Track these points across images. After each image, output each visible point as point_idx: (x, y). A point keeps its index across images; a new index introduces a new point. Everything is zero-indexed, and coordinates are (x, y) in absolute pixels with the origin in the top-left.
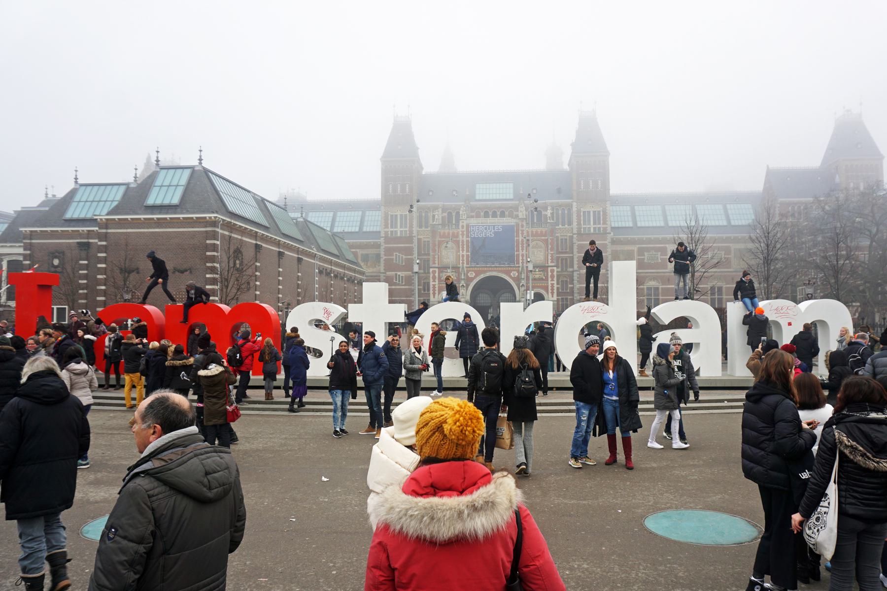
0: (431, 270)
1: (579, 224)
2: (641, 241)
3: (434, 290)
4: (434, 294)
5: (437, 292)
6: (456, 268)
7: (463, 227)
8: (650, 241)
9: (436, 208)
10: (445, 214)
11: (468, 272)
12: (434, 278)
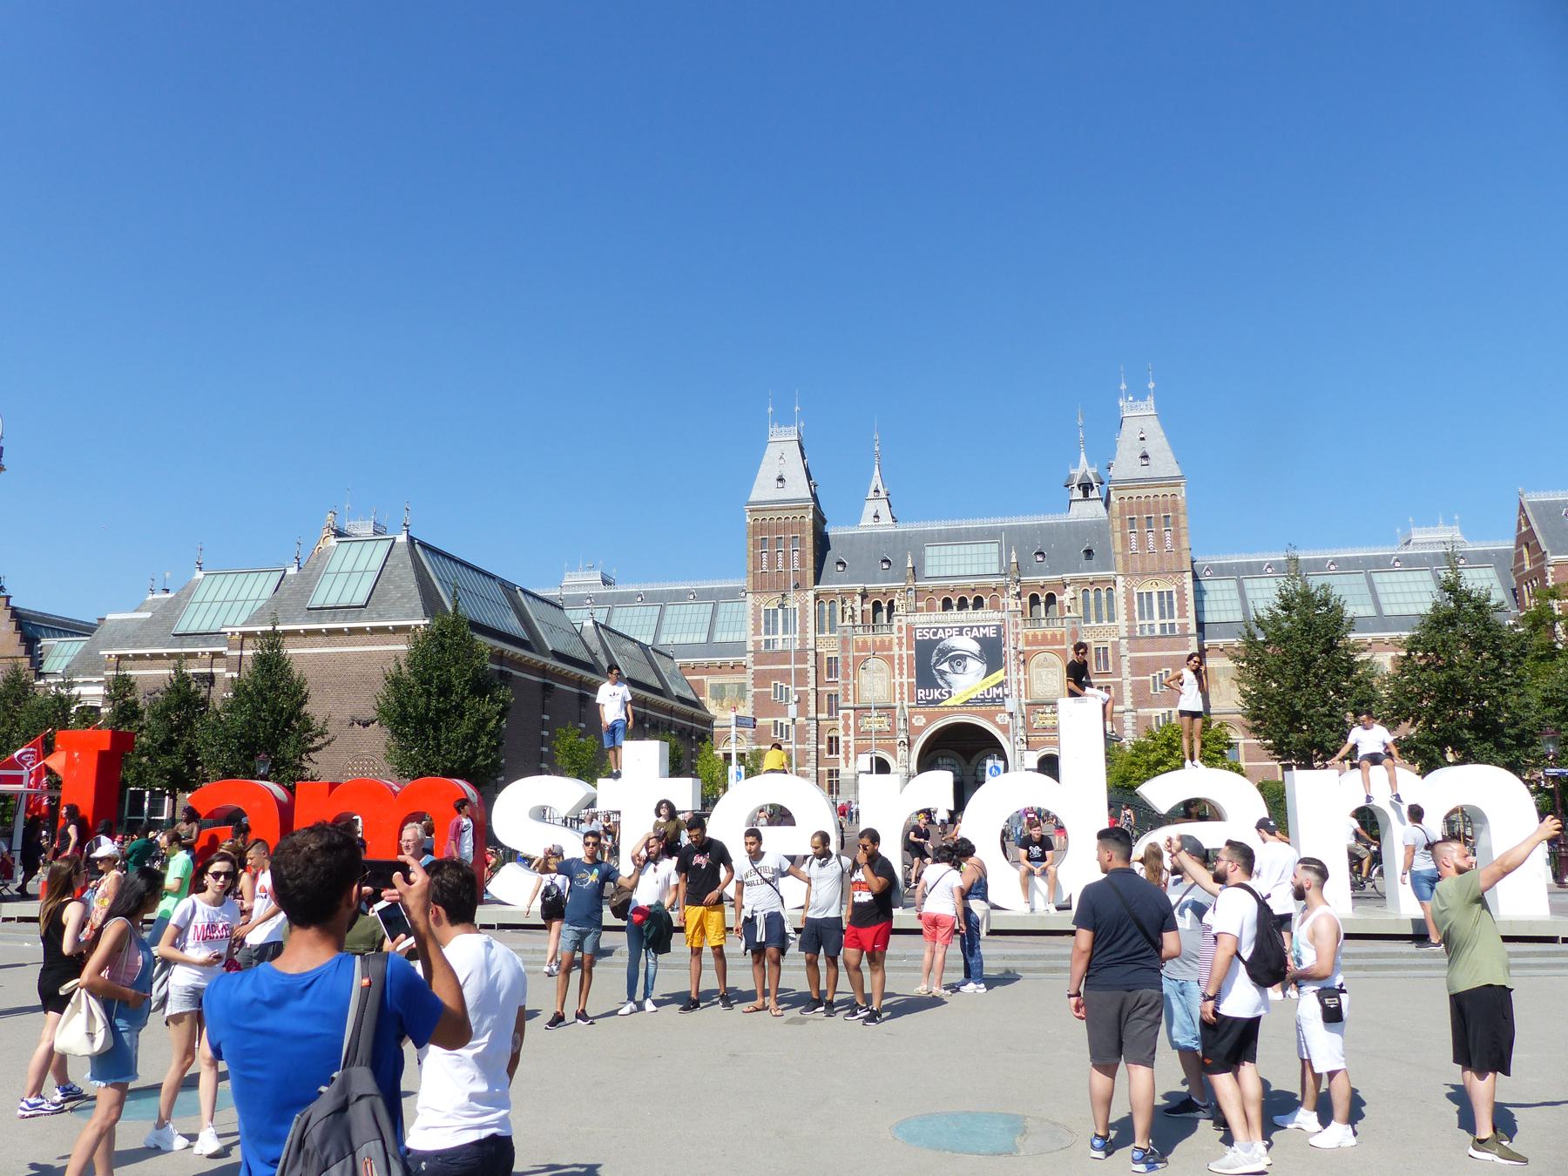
0: (841, 712)
1: (1131, 618)
3: (847, 753)
4: (847, 759)
5: (852, 755)
6: (888, 709)
7: (900, 629)
9: (852, 593)
10: (869, 606)
11: (911, 715)
12: (846, 728)
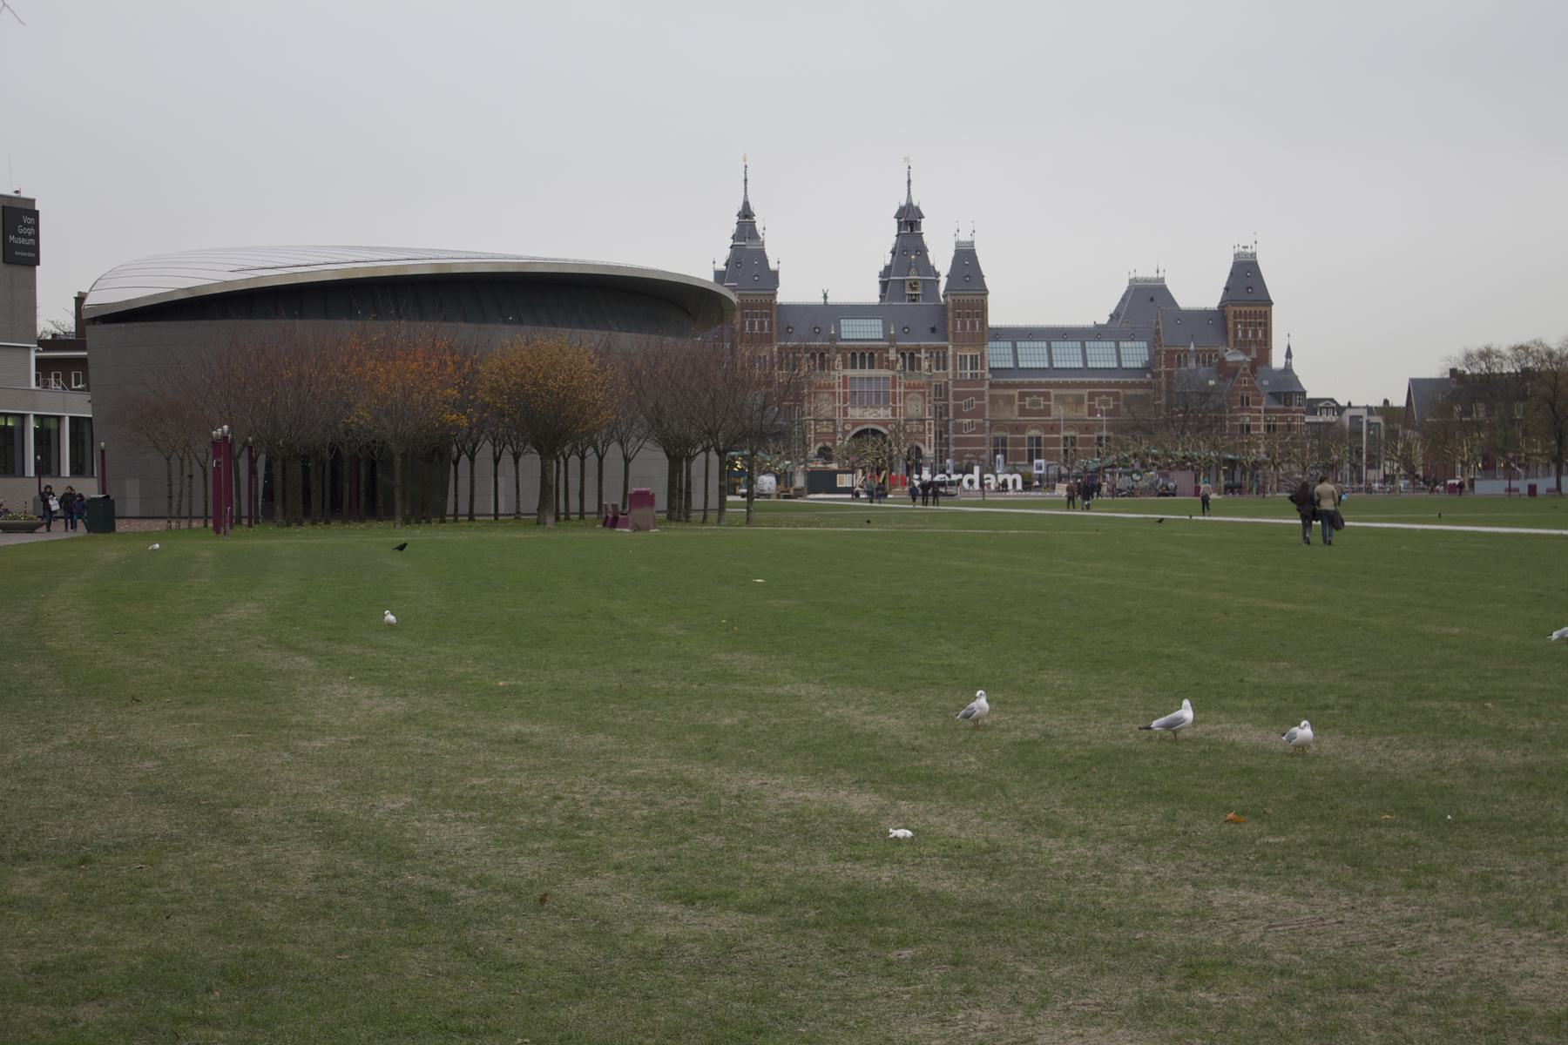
2: (1021, 385)
8: (1032, 385)
